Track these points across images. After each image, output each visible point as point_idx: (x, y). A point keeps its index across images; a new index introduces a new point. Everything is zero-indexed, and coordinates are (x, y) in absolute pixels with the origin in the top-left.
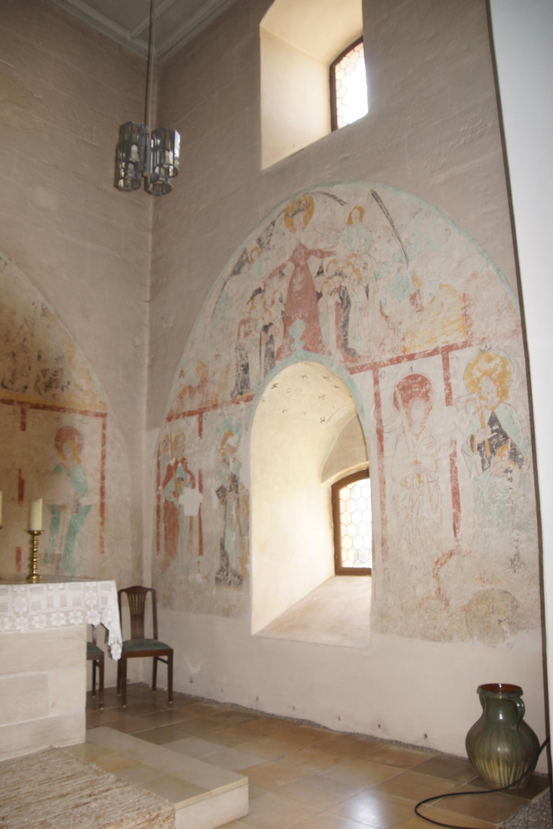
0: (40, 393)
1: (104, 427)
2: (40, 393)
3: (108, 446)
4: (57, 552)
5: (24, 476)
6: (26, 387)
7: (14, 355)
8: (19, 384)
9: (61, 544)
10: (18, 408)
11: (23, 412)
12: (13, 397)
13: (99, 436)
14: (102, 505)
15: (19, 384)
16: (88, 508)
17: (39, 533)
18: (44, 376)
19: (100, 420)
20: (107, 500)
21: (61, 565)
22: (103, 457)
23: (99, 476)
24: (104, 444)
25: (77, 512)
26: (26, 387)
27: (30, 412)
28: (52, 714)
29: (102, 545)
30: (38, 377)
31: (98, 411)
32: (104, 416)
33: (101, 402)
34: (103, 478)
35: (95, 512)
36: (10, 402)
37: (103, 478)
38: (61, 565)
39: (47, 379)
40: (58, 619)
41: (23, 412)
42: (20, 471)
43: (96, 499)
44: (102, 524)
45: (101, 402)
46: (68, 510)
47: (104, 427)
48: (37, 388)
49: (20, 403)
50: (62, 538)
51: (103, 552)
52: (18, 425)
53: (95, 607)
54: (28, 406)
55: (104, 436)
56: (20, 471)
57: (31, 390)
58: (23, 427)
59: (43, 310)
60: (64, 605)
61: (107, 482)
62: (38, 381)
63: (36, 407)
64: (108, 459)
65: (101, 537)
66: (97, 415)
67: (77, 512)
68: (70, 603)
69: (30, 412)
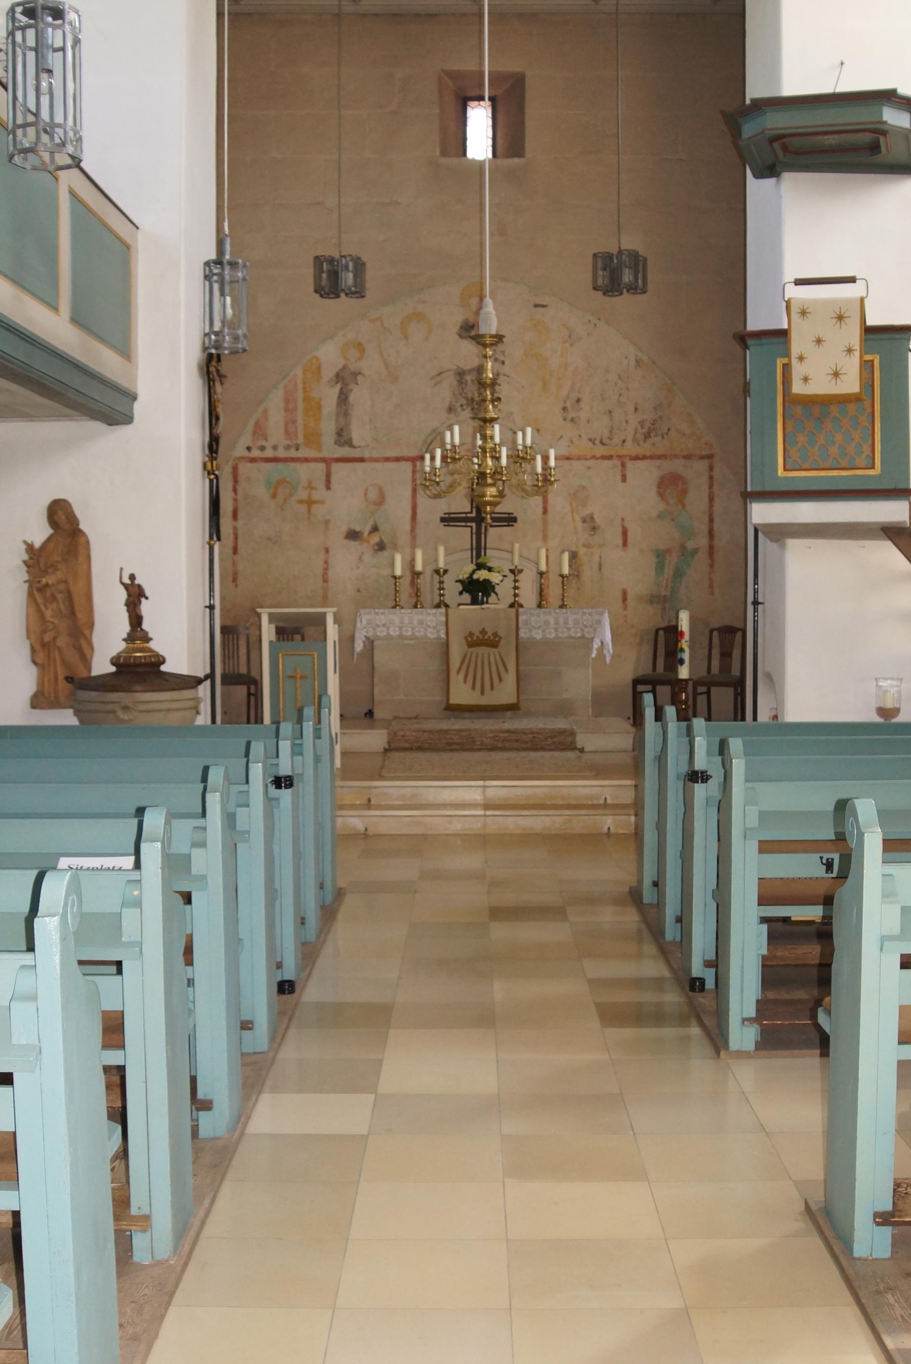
0: (639, 445)
1: (711, 468)
2: (639, 445)
3: (716, 488)
4: (663, 593)
5: (627, 524)
6: (624, 441)
7: (610, 412)
8: (617, 440)
9: (667, 586)
10: (618, 463)
11: (623, 465)
12: (613, 453)
13: (705, 479)
14: (711, 548)
15: (617, 440)
16: (696, 551)
17: (400, 578)
18: (642, 427)
19: (706, 463)
20: (717, 542)
21: (667, 605)
22: (711, 499)
23: (706, 519)
24: (711, 486)
25: (683, 555)
26: (624, 441)
27: (630, 465)
28: (565, 696)
29: (711, 586)
30: (636, 429)
31: (704, 453)
32: (710, 457)
33: (706, 444)
34: (711, 520)
35: (703, 556)
36: (610, 458)
37: (711, 520)
38: (667, 605)
39: (645, 430)
40: (563, 632)
41: (623, 465)
42: (623, 520)
43: (703, 542)
44: (712, 566)
45: (706, 444)
46: (674, 554)
47: (711, 468)
48: (635, 440)
49: (619, 457)
50: (667, 580)
51: (712, 593)
52: (619, 477)
53: (591, 626)
54: (628, 458)
55: (711, 478)
56: (623, 520)
57: (629, 443)
58: (624, 479)
59: (637, 361)
60: (566, 623)
61: (716, 526)
62: (636, 433)
63: (636, 458)
64: (717, 502)
65: (710, 579)
66: (702, 457)
67: (683, 555)
68: (571, 622)
69: (630, 465)
